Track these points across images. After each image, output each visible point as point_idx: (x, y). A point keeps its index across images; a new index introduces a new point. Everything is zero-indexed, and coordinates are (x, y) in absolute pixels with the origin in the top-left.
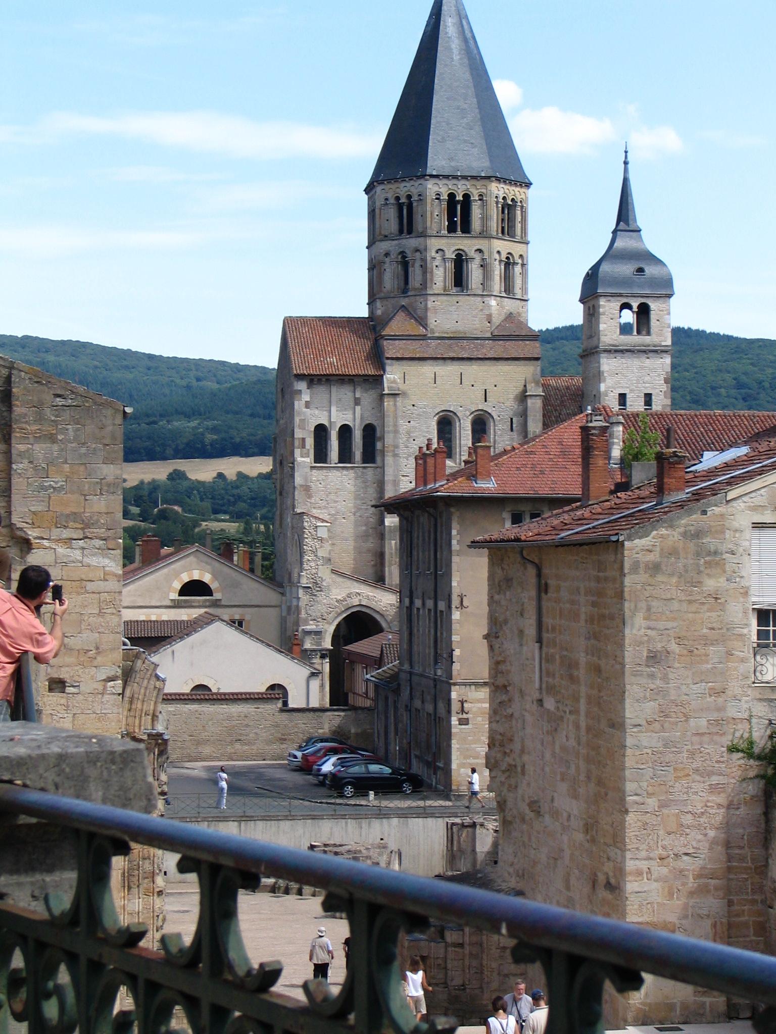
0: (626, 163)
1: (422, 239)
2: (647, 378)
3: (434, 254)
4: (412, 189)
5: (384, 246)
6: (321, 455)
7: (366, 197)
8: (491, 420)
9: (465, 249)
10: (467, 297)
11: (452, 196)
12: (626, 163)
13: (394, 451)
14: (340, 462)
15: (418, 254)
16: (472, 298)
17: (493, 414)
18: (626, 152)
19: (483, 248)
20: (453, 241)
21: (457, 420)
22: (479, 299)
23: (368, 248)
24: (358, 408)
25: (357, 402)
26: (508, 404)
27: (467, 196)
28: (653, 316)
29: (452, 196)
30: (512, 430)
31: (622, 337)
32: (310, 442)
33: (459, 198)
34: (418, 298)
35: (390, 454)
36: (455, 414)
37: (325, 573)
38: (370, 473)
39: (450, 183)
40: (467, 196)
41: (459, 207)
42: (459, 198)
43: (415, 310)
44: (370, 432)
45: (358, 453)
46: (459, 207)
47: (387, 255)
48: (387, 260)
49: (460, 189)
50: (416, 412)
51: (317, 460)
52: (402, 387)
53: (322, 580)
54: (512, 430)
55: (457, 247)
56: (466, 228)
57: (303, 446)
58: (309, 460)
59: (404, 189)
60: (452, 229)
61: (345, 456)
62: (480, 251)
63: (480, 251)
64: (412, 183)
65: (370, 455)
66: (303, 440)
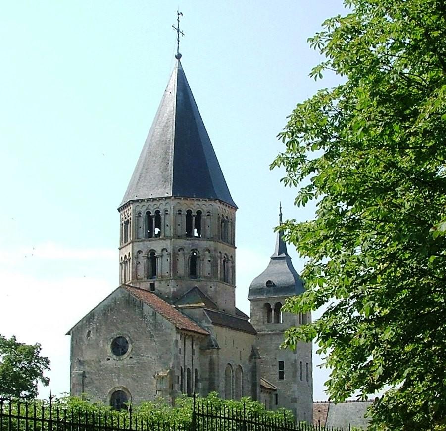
4: (204, 207)
34: (208, 283)
39: (224, 207)
43: (207, 291)
47: (181, 249)
64: (204, 202)
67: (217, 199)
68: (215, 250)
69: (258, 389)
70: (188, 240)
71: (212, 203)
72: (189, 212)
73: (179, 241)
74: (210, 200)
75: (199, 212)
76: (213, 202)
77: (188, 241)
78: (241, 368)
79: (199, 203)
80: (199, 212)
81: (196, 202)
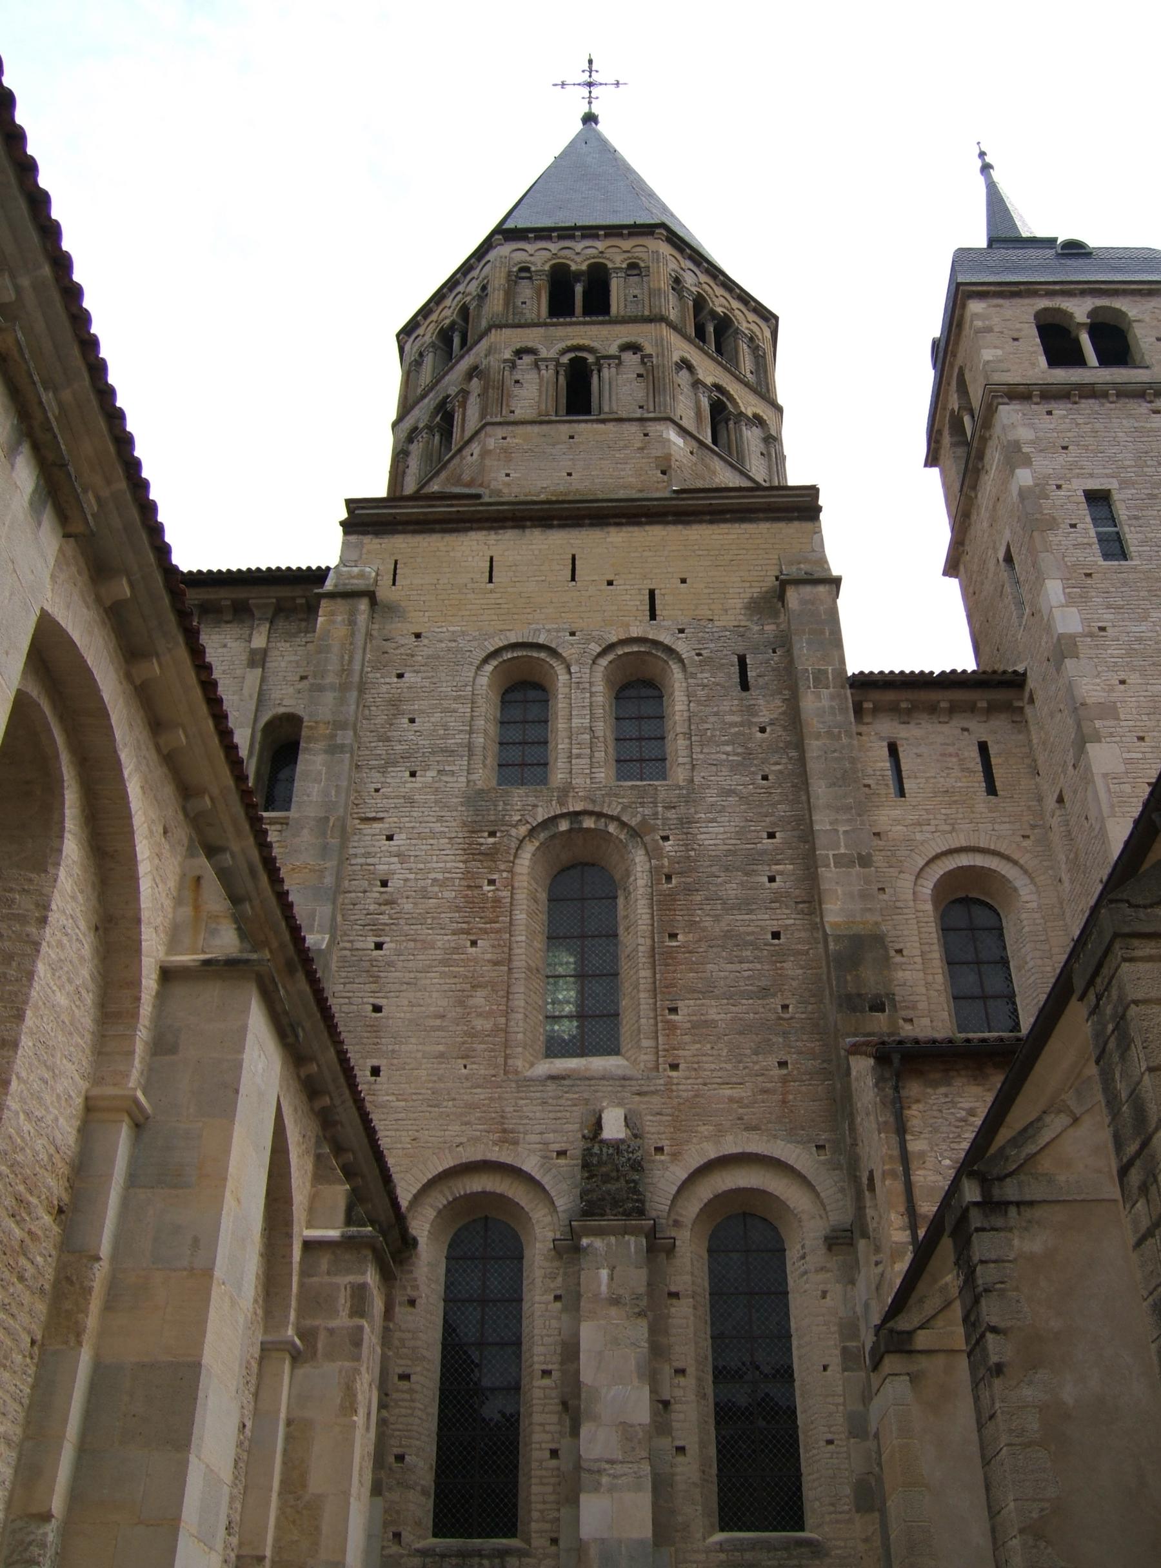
0: (986, 168)
8: (675, 667)
9: (593, 344)
10: (601, 426)
13: (333, 736)
16: (610, 426)
17: (681, 647)
20: (560, 331)
21: (560, 669)
22: (633, 428)
26: (728, 620)
30: (745, 685)
35: (319, 746)
39: (554, 247)
41: (579, 289)
46: (579, 289)
49: (580, 255)
50: (427, 652)
54: (745, 685)
78: (669, 650)
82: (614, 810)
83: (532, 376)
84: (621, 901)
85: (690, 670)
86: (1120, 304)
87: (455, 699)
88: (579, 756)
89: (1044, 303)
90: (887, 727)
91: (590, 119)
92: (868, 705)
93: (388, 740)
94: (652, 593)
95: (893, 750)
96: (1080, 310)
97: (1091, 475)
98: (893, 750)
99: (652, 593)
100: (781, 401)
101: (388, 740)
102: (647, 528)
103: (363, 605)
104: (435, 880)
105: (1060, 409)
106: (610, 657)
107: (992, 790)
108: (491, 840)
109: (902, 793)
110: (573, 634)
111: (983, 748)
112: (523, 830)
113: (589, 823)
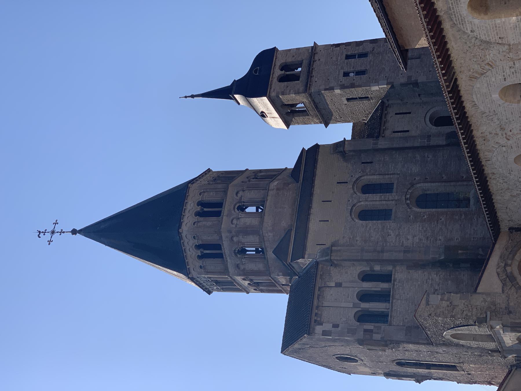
0: (193, 96)
1: (224, 235)
2: (334, 59)
3: (234, 226)
4: (191, 243)
5: (231, 269)
6: (382, 317)
7: (215, 293)
8: (362, 178)
9: (234, 203)
11: (198, 214)
12: (193, 96)
14: (389, 303)
15: (235, 239)
18: (186, 97)
19: (236, 191)
23: (248, 293)
24: (344, 285)
25: (339, 285)
27: (201, 204)
28: (290, 60)
29: (198, 214)
31: (301, 79)
32: (369, 326)
33: (199, 208)
34: (266, 239)
36: (354, 205)
37: (478, 300)
38: (400, 274)
40: (201, 204)
41: (205, 209)
42: (199, 208)
44: (366, 277)
45: (384, 286)
46: (205, 209)
47: (238, 266)
48: (242, 267)
51: (386, 322)
52: (328, 245)
53: (485, 301)
55: (232, 209)
56: (220, 205)
57: (371, 331)
58: (383, 326)
59: (191, 254)
60: (218, 214)
61: (384, 296)
62: (237, 193)
63: (237, 193)
64: (186, 244)
65: (387, 278)
66: (366, 331)
67: (179, 232)
68: (230, 232)
69: (382, 144)
70: (227, 261)
71: (184, 235)
72: (200, 257)
73: (230, 270)
74: (181, 238)
75: (198, 247)
76: (182, 234)
77: (229, 260)
78: (357, 179)
79: (188, 248)
80: (198, 247)
81: (188, 252)
82: (406, 190)
83: (242, 220)
84: (428, 192)
85: (365, 174)
86: (278, 64)
87: (366, 227)
88: (388, 198)
89: (275, 80)
90: (388, 133)
91: (74, 232)
92: (383, 135)
93: (378, 242)
94: (338, 183)
95: (394, 132)
96: (277, 72)
97: (339, 75)
98: (394, 132)
99: (338, 183)
100: (244, 169)
101: (378, 242)
102: (316, 184)
103: (333, 248)
104: (422, 228)
105: (314, 79)
106: (357, 193)
107: (410, 113)
108: (411, 217)
109: (408, 131)
110: (349, 201)
111: (396, 114)
112: (409, 210)
113: (408, 196)
